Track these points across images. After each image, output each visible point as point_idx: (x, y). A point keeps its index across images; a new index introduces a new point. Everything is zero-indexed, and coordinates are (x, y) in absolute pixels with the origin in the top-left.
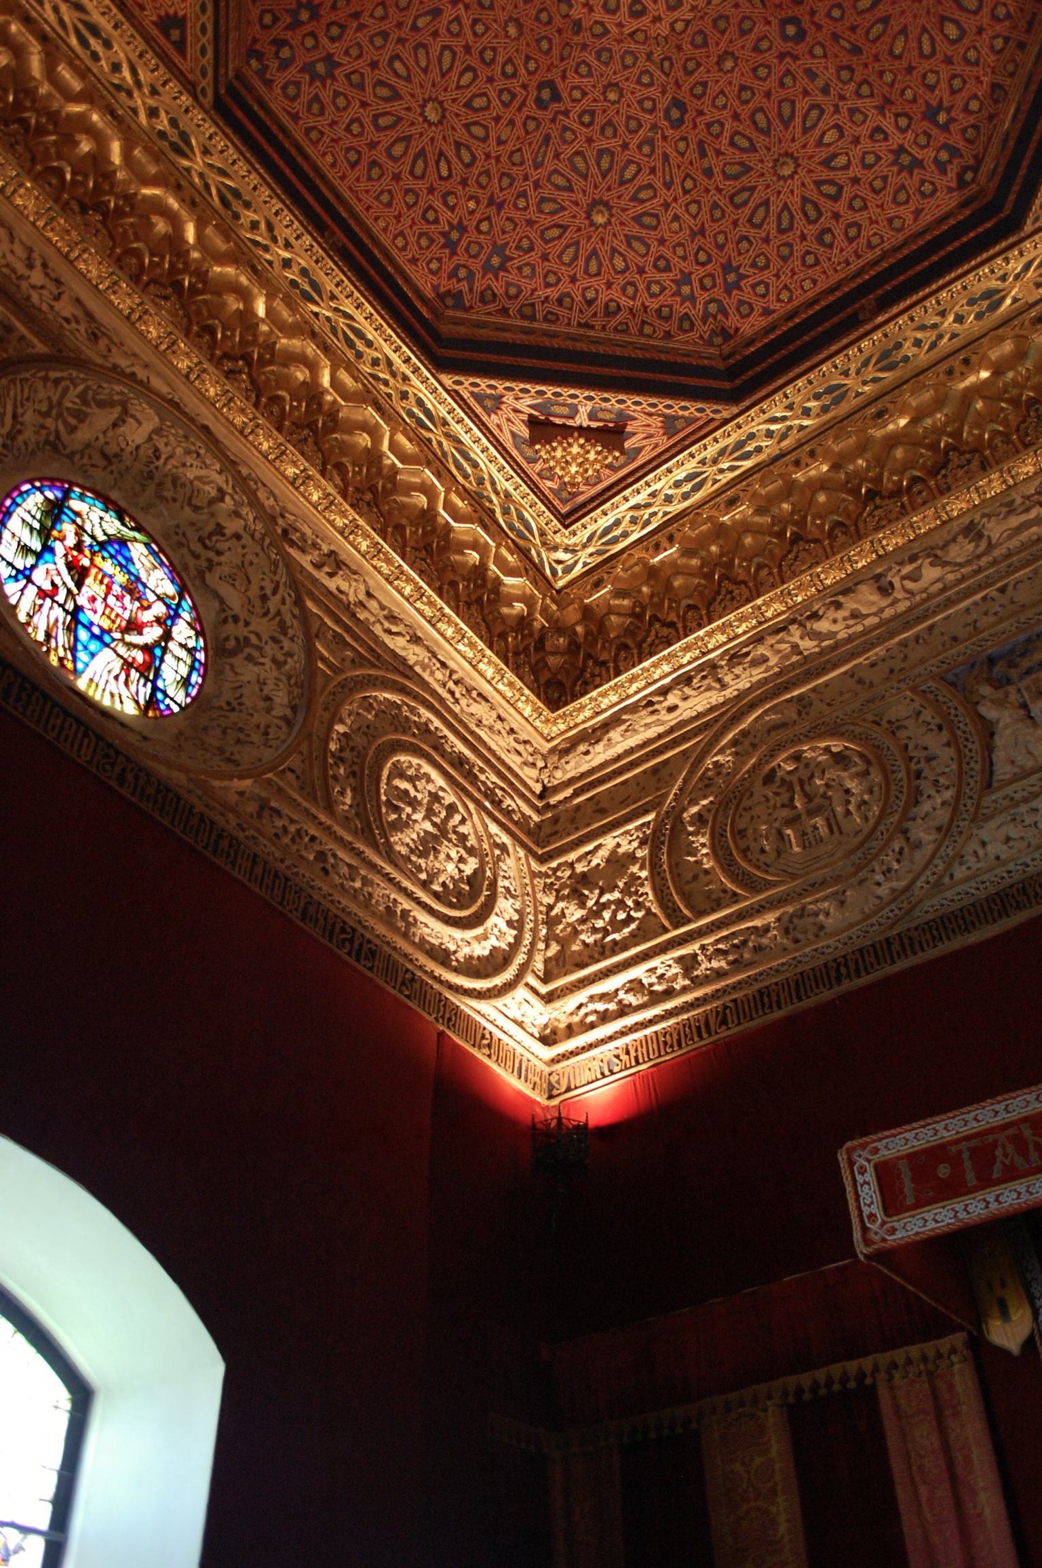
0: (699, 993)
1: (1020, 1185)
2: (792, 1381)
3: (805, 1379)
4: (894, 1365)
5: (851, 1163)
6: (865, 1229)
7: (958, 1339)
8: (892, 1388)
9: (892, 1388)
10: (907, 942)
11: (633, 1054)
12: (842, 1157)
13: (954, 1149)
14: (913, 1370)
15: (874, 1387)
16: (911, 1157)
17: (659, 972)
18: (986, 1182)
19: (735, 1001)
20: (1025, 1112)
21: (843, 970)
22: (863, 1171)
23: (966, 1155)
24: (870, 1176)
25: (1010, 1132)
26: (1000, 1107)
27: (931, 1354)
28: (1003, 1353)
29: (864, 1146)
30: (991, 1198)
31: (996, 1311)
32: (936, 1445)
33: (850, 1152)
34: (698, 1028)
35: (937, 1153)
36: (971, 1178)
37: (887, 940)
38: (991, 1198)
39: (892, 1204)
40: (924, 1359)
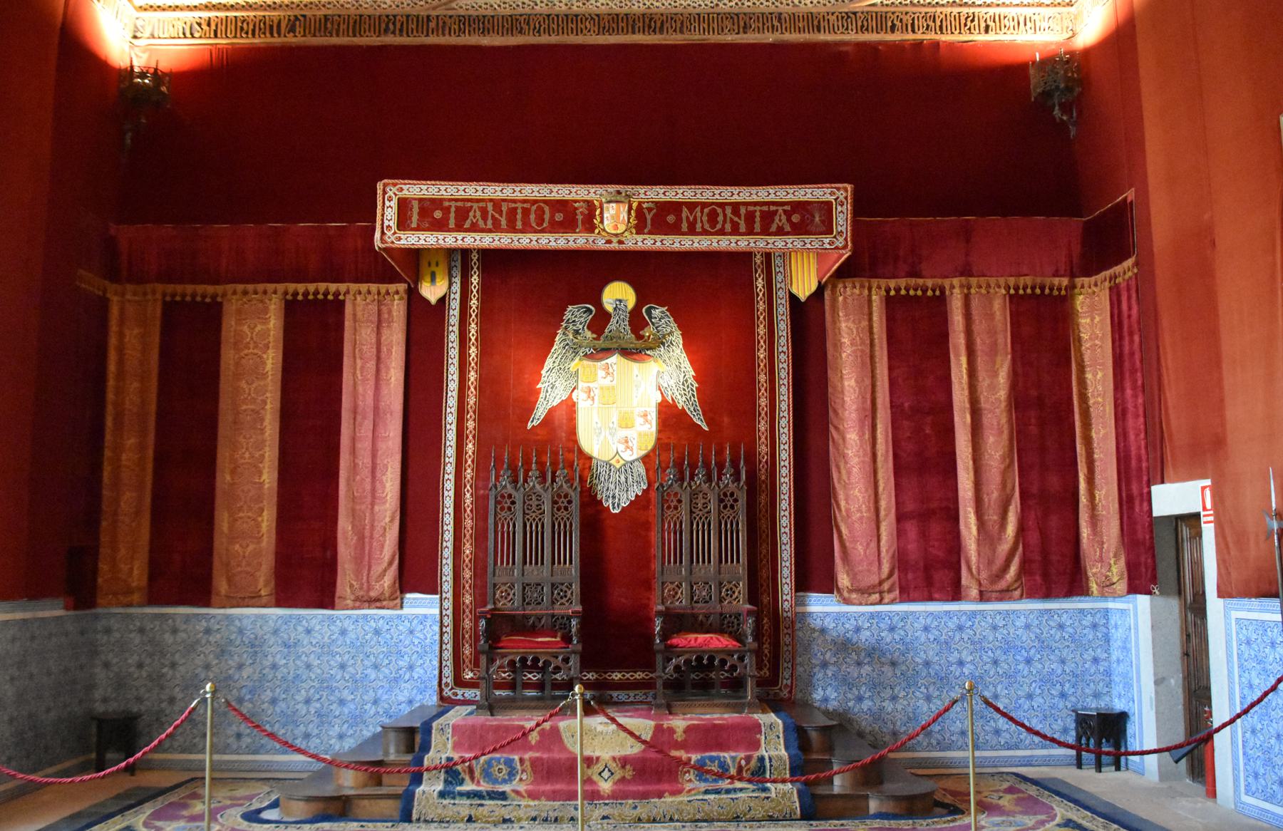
1: (477, 236)
2: (292, 287)
3: (301, 288)
4: (360, 293)
5: (385, 193)
6: (383, 233)
7: (402, 287)
8: (354, 305)
9: (354, 305)
10: (442, 25)
11: (213, 27)
12: (380, 186)
13: (447, 204)
14: (370, 298)
15: (344, 301)
16: (420, 200)
18: (459, 228)
19: (304, 16)
20: (493, 196)
21: (391, 26)
22: (390, 199)
23: (453, 209)
24: (394, 203)
25: (482, 204)
26: (480, 188)
27: (383, 291)
28: (427, 302)
29: (395, 185)
30: (460, 238)
31: (428, 278)
32: (374, 340)
33: (385, 185)
34: (271, 27)
35: (437, 203)
36: (452, 225)
37: (428, 17)
38: (460, 238)
39: (403, 224)
40: (379, 293)
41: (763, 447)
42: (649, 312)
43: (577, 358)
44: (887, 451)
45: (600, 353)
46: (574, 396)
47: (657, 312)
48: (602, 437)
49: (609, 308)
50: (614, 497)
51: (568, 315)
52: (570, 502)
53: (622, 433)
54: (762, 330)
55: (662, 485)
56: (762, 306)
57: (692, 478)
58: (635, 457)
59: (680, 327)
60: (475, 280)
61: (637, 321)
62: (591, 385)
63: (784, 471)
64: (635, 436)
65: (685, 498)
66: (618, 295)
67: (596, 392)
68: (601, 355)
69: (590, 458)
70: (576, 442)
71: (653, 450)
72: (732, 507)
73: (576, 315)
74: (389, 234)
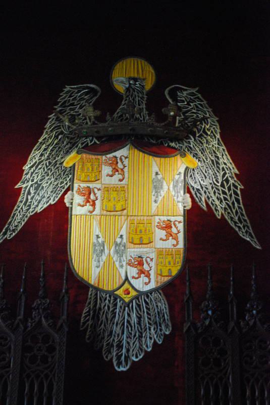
42: (173, 94)
43: (73, 154)
45: (104, 142)
46: (66, 201)
47: (183, 95)
48: (104, 257)
49: (121, 88)
50: (120, 346)
51: (63, 97)
52: (51, 349)
53: (133, 251)
55: (194, 324)
57: (241, 316)
59: (216, 113)
61: (155, 101)
62: (91, 185)
64: (153, 255)
66: (131, 74)
67: (99, 194)
69: (82, 286)
71: (181, 274)
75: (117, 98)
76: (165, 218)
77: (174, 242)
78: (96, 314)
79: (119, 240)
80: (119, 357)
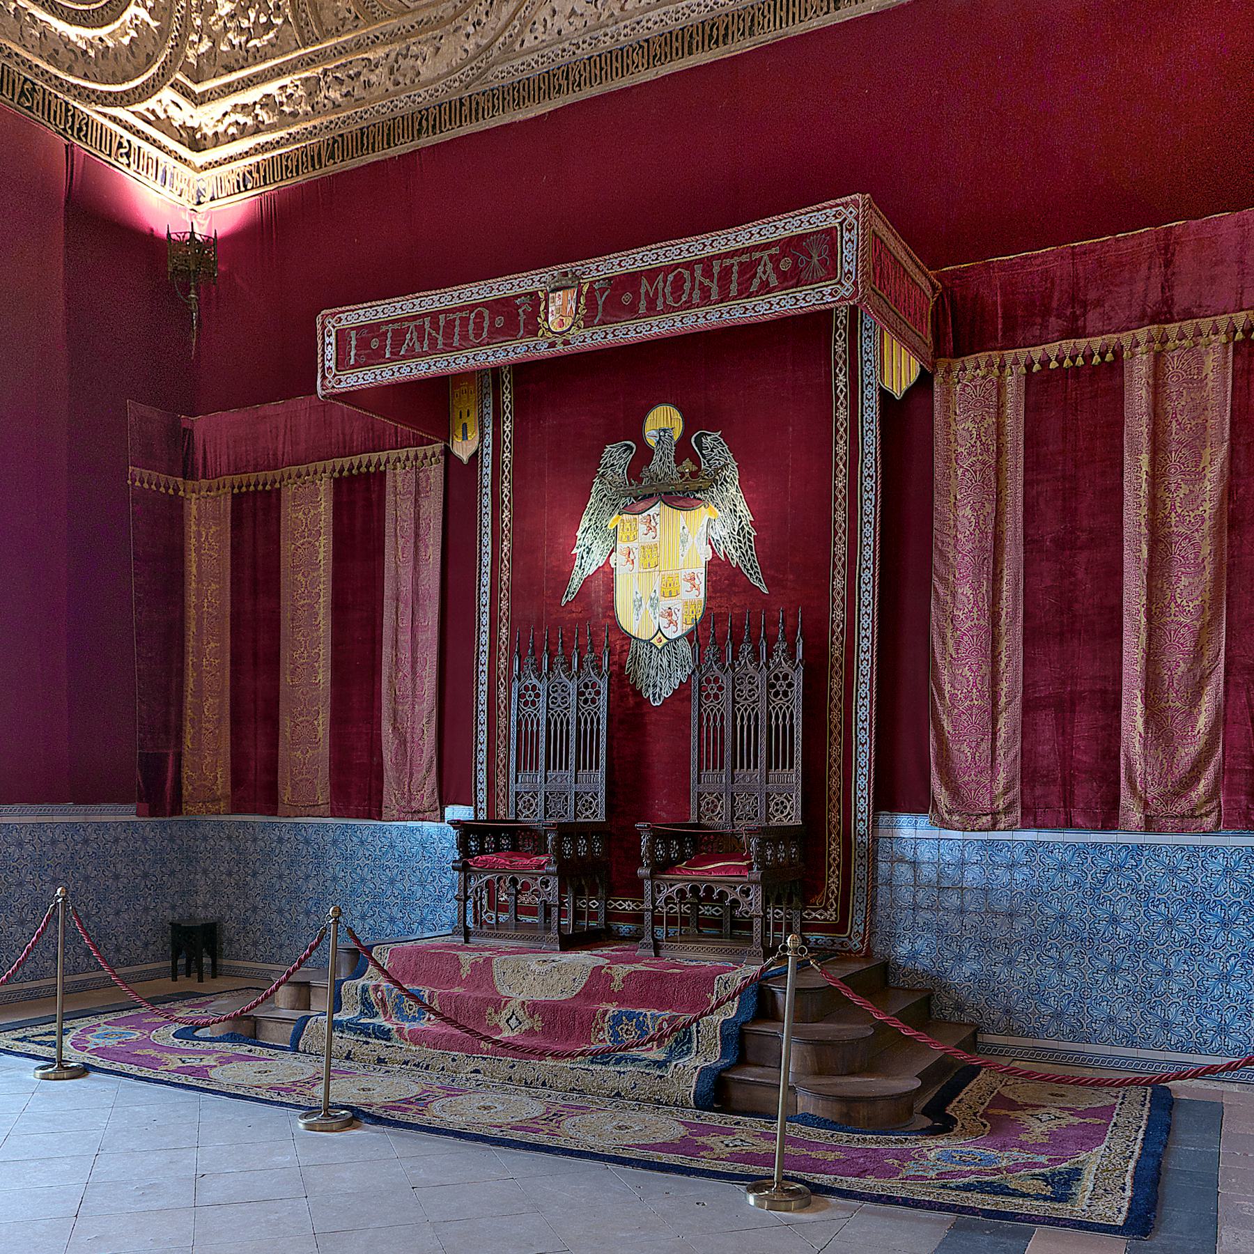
0: (316, 122)
1: (412, 363)
5: (324, 328)
6: (324, 377)
12: (319, 319)
17: (289, 91)
18: (396, 356)
19: (342, 135)
24: (332, 339)
39: (341, 363)
41: (839, 612)
43: (616, 516)
44: (1015, 610)
47: (707, 441)
49: (652, 442)
50: (655, 686)
51: (606, 459)
53: (665, 603)
54: (841, 448)
56: (842, 414)
58: (679, 633)
60: (508, 427)
61: (683, 450)
63: (865, 644)
65: (726, 681)
66: (663, 421)
68: (642, 505)
70: (614, 618)
72: (785, 694)
73: (616, 456)
74: (330, 377)
75: (651, 452)
76: (690, 571)
77: (695, 592)
78: (636, 660)
79: (653, 595)
80: (654, 695)
